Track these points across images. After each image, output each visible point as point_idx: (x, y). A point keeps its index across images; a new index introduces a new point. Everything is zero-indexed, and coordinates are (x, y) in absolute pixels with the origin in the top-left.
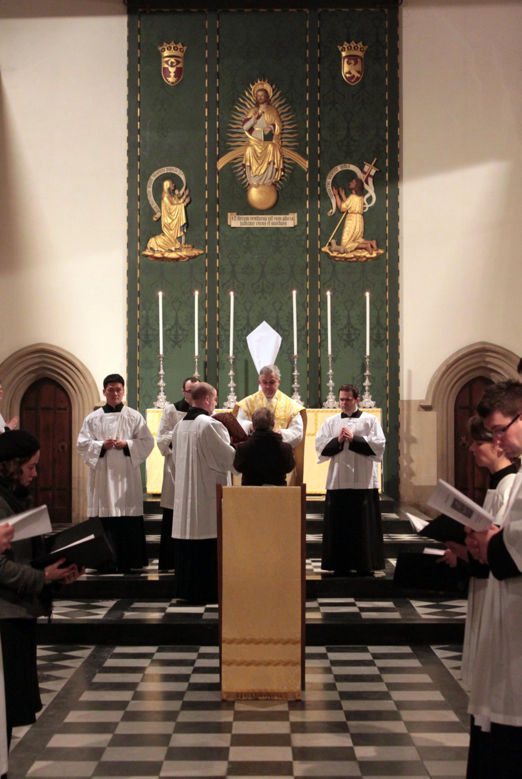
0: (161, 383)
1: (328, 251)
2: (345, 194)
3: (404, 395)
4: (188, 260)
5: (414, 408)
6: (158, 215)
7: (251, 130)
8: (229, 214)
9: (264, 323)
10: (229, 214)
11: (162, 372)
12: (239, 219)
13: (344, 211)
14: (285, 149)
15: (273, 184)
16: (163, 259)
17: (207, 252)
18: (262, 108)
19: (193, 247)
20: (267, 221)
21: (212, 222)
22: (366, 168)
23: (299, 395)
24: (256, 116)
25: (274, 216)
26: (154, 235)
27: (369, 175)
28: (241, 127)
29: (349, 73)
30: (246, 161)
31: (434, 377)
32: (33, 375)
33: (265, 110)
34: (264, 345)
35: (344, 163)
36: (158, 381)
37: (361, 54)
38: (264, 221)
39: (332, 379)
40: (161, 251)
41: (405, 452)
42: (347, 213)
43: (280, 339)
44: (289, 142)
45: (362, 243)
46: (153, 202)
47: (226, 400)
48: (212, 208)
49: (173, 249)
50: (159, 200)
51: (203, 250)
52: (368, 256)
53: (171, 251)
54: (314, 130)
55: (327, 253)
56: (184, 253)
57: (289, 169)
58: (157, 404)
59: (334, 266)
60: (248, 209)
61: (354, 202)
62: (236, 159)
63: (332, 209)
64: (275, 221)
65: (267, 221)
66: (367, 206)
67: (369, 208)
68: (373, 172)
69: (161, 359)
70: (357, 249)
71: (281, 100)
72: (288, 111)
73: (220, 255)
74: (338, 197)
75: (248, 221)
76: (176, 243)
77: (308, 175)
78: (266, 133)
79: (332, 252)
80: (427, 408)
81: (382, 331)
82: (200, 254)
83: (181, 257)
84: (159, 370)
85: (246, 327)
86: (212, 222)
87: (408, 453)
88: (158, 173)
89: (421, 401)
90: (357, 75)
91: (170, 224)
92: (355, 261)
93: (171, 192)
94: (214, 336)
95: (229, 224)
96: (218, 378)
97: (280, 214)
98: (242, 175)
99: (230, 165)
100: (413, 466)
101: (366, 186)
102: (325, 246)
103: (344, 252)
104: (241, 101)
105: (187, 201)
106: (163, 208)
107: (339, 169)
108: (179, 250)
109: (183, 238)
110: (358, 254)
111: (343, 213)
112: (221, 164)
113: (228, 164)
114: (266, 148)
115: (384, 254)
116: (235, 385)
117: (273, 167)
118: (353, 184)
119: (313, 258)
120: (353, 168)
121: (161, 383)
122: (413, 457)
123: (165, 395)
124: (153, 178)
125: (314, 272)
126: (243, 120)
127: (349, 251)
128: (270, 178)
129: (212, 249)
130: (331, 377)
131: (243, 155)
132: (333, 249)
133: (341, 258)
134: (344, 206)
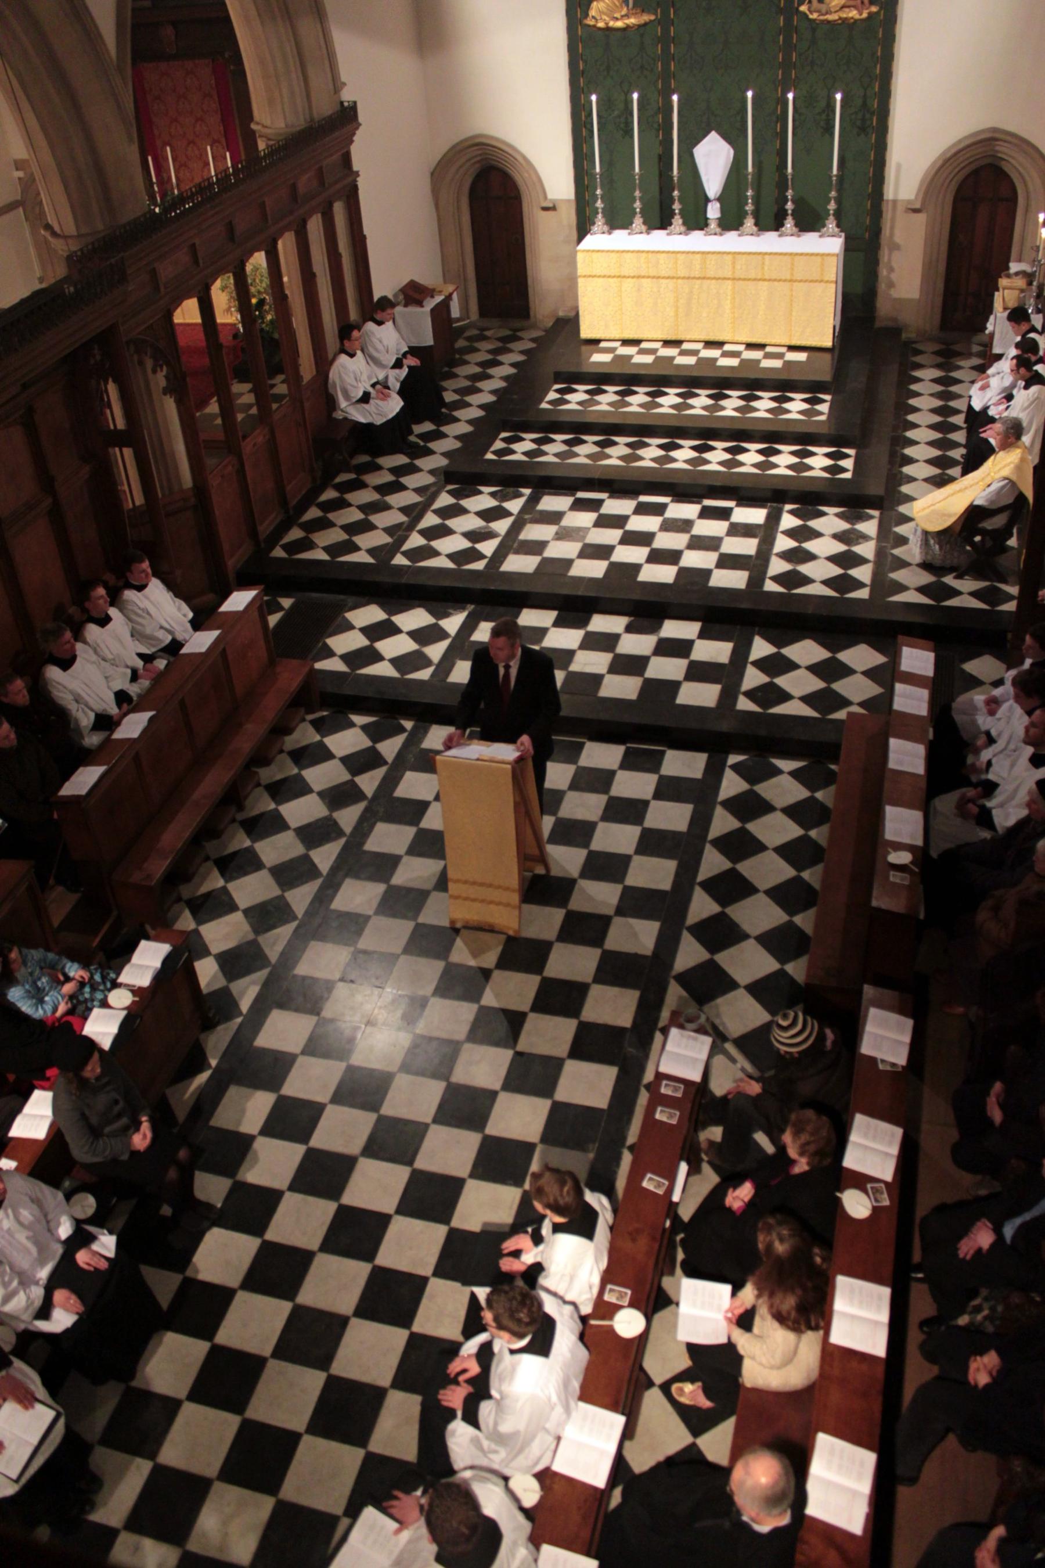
3: (889, 193)
5: (900, 208)
9: (713, 135)
16: (608, 29)
19: (643, 11)
31: (935, 162)
32: (477, 165)
34: (713, 159)
36: (596, 201)
41: (886, 259)
43: (732, 152)
53: (617, 19)
56: (632, 21)
58: (595, 228)
59: (814, 30)
73: (676, 21)
80: (916, 211)
81: (868, 116)
82: (651, 21)
85: (691, 140)
87: (890, 260)
89: (909, 202)
100: (894, 277)
103: (827, 13)
108: (627, 16)
115: (878, 13)
119: (788, 21)
122: (894, 264)
125: (788, 39)
132: (812, 9)
133: (823, 21)
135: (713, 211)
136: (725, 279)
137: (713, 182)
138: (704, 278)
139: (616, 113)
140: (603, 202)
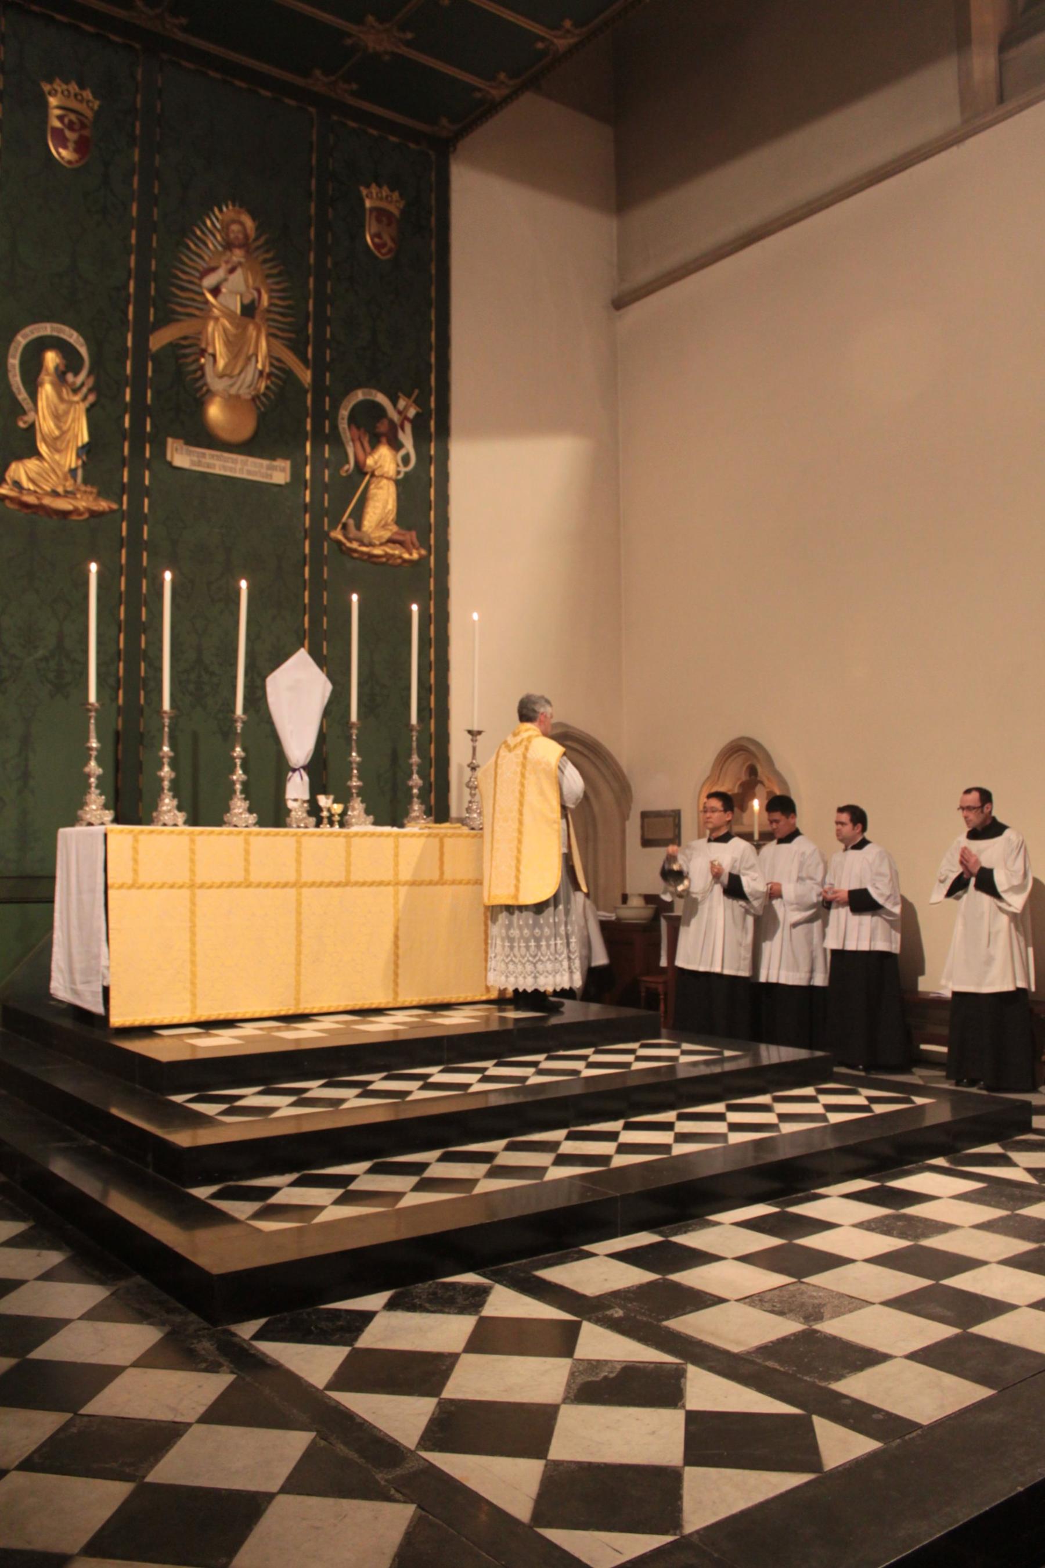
0: (93, 767)
1: (340, 537)
2: (370, 442)
4: (87, 520)
6: (30, 417)
7: (216, 291)
8: (170, 440)
10: (170, 440)
11: (94, 744)
12: (189, 453)
13: (369, 470)
14: (273, 341)
15: (255, 399)
16: (40, 508)
17: (125, 507)
18: (238, 255)
20: (239, 466)
21: (137, 450)
22: (402, 403)
23: (362, 802)
24: (229, 266)
25: (251, 460)
26: (20, 457)
27: (406, 418)
28: (196, 281)
29: (378, 235)
30: (207, 344)
33: (242, 260)
34: (298, 697)
35: (366, 387)
37: (396, 212)
38: (233, 465)
39: (418, 773)
40: (35, 492)
42: (373, 475)
43: (329, 687)
44: (279, 329)
45: (396, 533)
46: (18, 389)
47: (228, 810)
48: (138, 423)
49: (60, 490)
50: (32, 387)
51: (116, 502)
52: (406, 556)
53: (55, 494)
54: (321, 321)
55: (339, 543)
56: (82, 504)
57: (277, 376)
60: (203, 437)
61: (384, 460)
62: (185, 338)
63: (348, 462)
64: (253, 469)
65: (239, 466)
66: (403, 470)
67: (406, 473)
68: (412, 412)
69: (93, 714)
70: (391, 541)
71: (267, 251)
72: (279, 274)
74: (358, 445)
75: (203, 460)
76: (66, 479)
77: (309, 397)
78: (247, 301)
79: (350, 540)
82: (112, 511)
83: (76, 511)
84: (87, 740)
85: (266, 660)
86: (137, 450)
88: (33, 333)
90: (390, 244)
91: (56, 438)
92: (383, 564)
93: (60, 376)
94: (204, 673)
95: (169, 458)
96: (141, 763)
97: (261, 457)
98: (195, 371)
99: (174, 348)
101: (401, 436)
102: (336, 528)
104: (198, 233)
105: (92, 398)
106: (42, 403)
107: (360, 395)
108: (68, 494)
109: (80, 473)
110: (389, 550)
111: (366, 474)
112: (157, 341)
113: (170, 344)
114: (245, 329)
116: (244, 777)
117: (256, 367)
118: (383, 427)
119: (316, 547)
120: (381, 398)
121: (93, 767)
123: (101, 794)
124: (22, 340)
125: (316, 573)
126: (201, 269)
127: (377, 543)
128: (249, 386)
129: (136, 504)
130: (415, 768)
131: (200, 333)
133: (362, 553)
134: (370, 461)
135: (297, 788)
136: (381, 883)
137: (299, 742)
138: (347, 884)
139: (41, 653)
140: (100, 762)
